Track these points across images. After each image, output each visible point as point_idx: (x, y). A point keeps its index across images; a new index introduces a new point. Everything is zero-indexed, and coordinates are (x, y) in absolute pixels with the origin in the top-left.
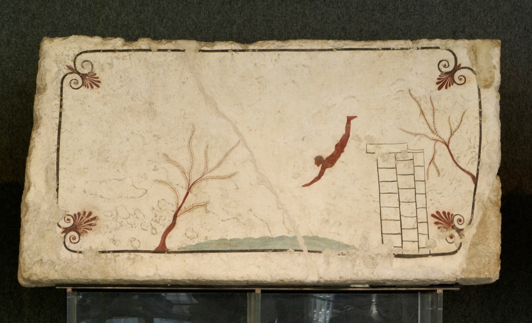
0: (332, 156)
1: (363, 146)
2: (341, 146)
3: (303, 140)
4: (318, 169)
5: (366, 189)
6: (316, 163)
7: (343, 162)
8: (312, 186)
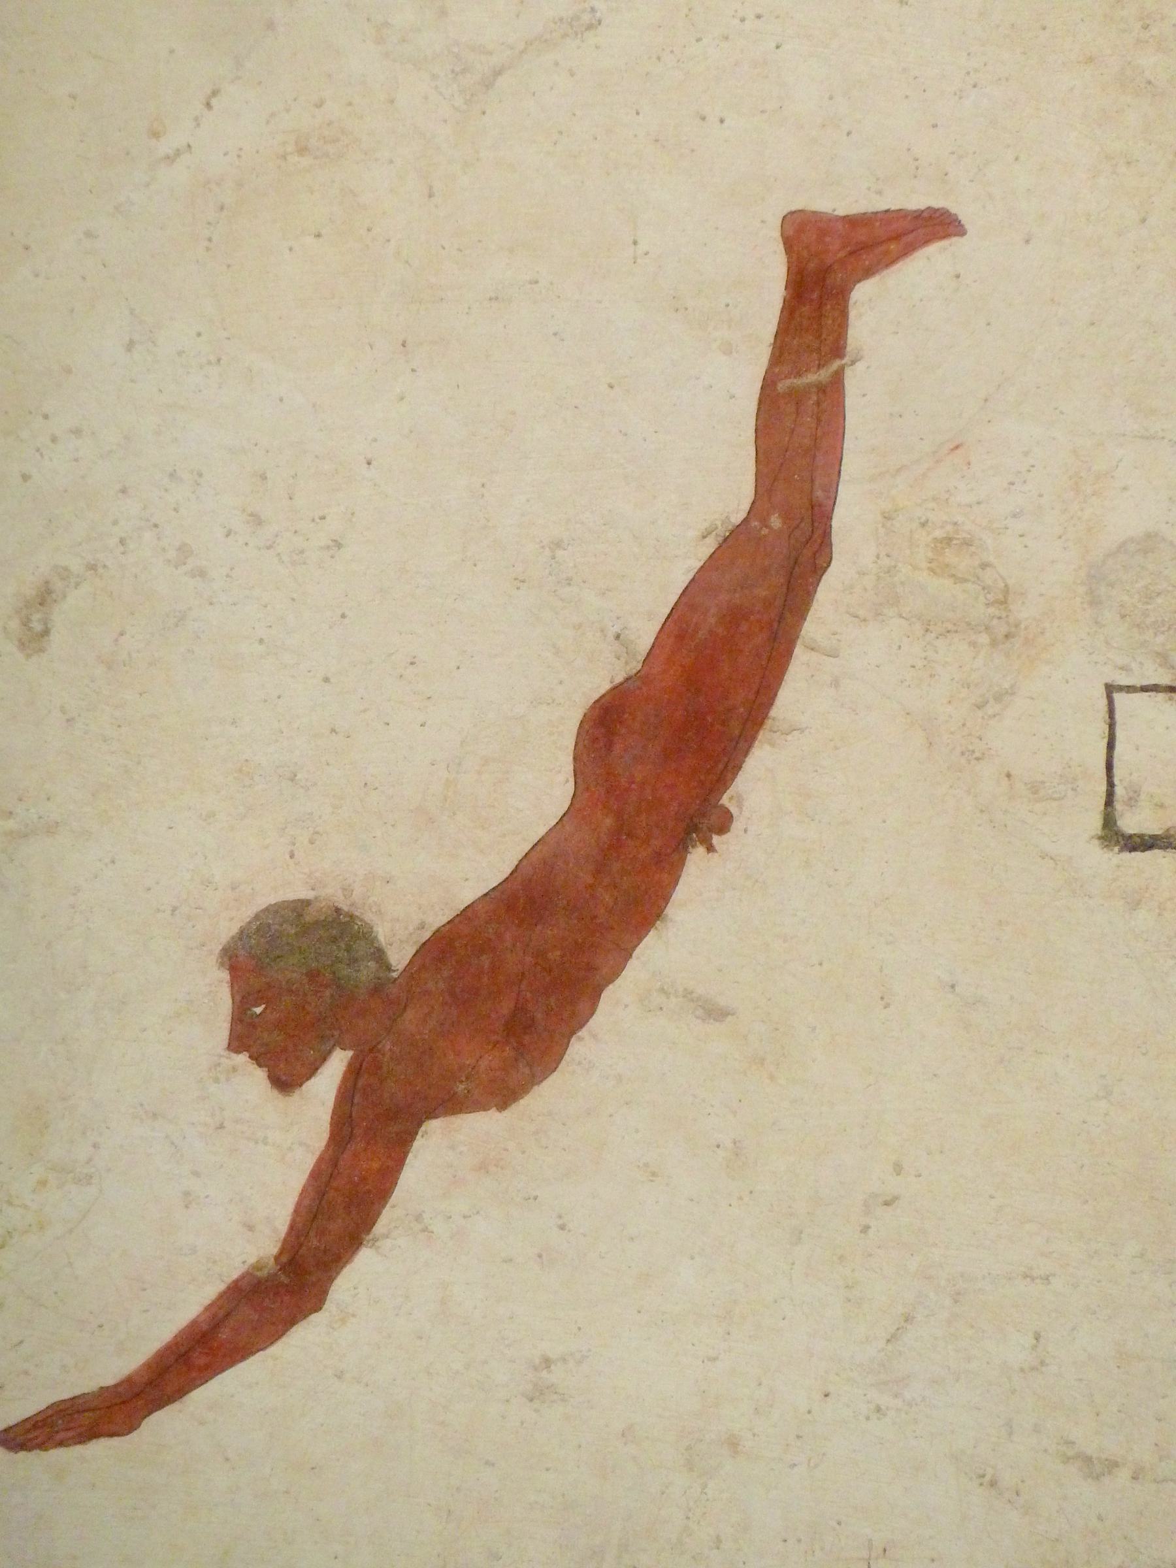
0: (525, 897)
1: (1053, 722)
2: (676, 736)
3: (34, 639)
4: (286, 1133)
5: (1097, 1468)
6: (243, 1038)
7: (715, 1013)
8: (164, 1424)
